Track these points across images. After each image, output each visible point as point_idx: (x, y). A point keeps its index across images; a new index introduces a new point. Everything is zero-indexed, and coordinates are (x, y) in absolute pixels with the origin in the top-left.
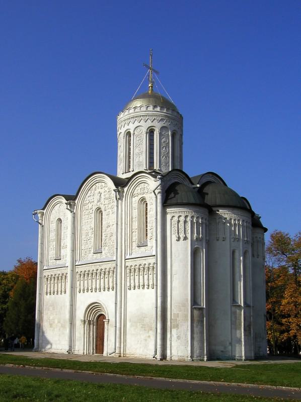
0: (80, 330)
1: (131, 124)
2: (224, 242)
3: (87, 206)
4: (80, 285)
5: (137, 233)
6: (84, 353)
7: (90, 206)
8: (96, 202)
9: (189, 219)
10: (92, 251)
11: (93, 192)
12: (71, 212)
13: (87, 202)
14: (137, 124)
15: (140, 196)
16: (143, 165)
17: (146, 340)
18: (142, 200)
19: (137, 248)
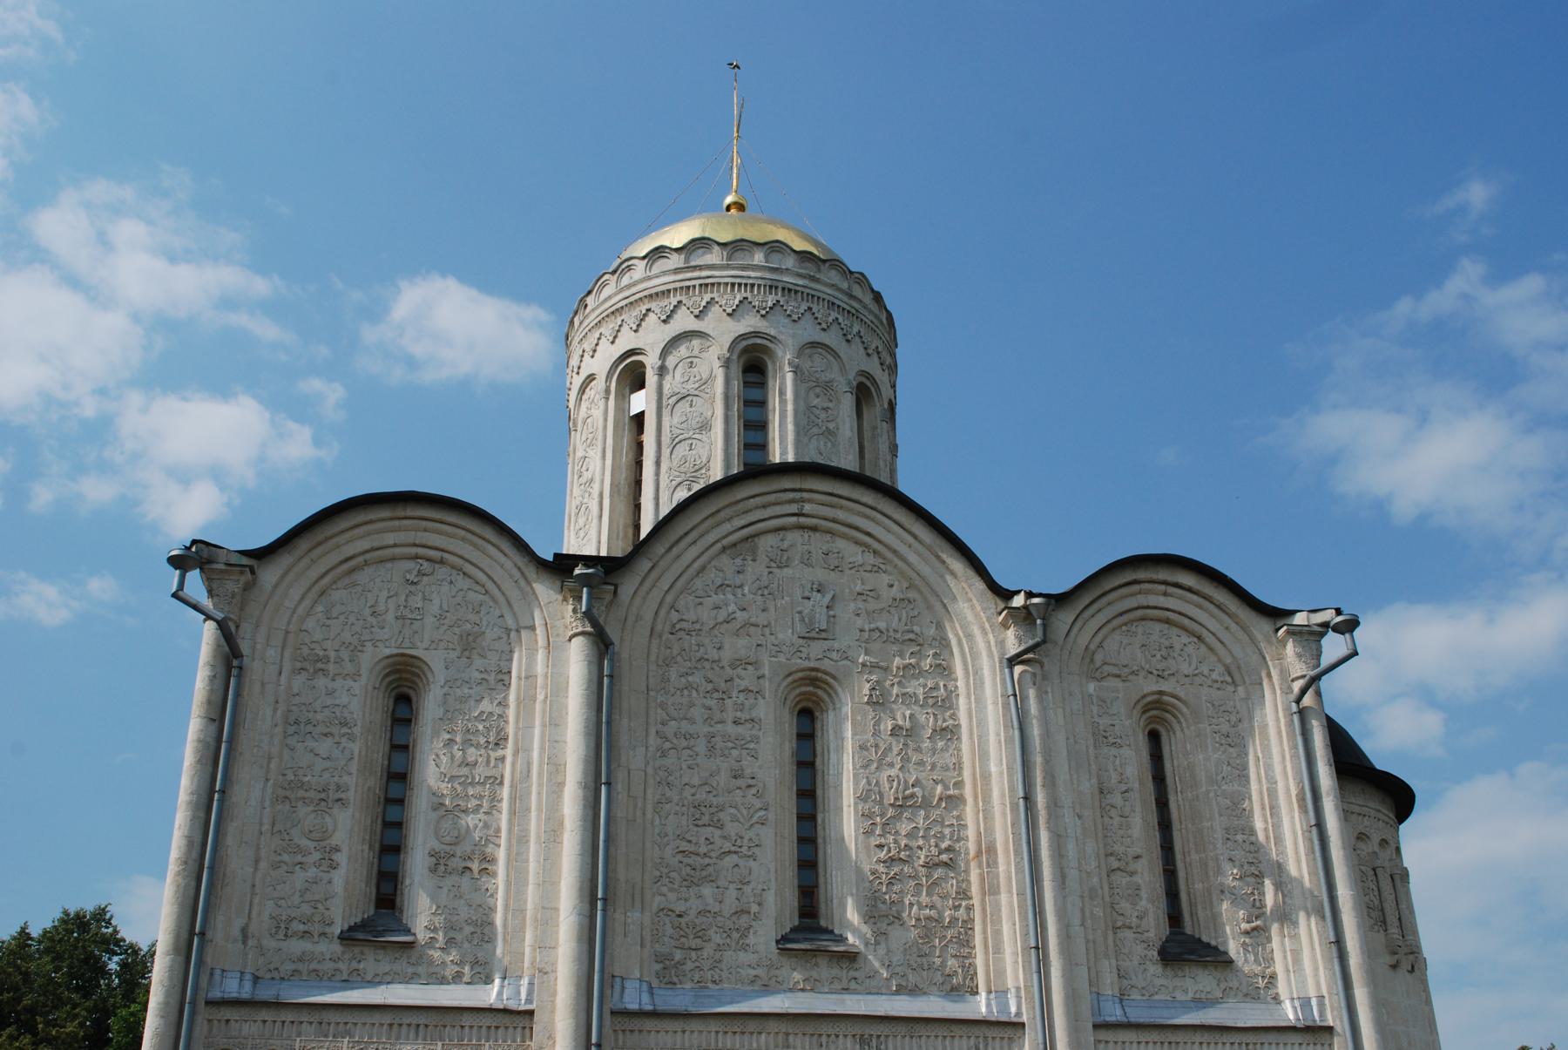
8: (786, 635)
11: (756, 570)
15: (1151, 686)
19: (1155, 969)
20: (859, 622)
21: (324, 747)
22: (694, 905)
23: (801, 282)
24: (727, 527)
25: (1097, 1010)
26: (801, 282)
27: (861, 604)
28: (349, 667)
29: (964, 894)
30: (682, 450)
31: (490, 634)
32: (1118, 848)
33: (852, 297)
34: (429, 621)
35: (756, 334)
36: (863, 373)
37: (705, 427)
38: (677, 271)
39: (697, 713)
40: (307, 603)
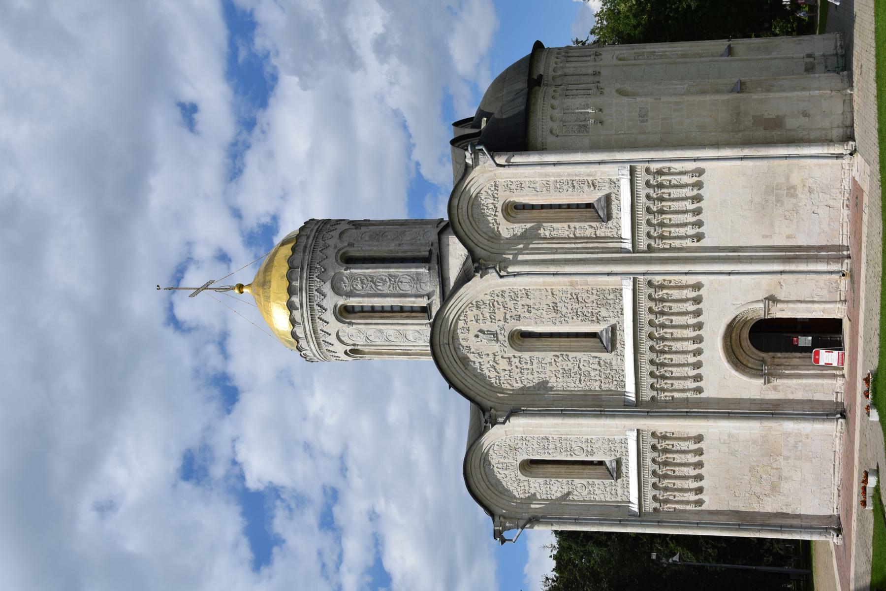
0: (792, 387)
1: (324, 303)
2: (603, 72)
3: (502, 374)
4: (683, 391)
5: (577, 225)
6: (840, 376)
7: (503, 364)
8: (496, 347)
9: (556, 103)
10: (605, 356)
12: (508, 418)
13: (493, 374)
14: (327, 288)
15: (500, 214)
16: (417, 274)
17: (811, 191)
18: (508, 214)
20: (488, 323)
21: (554, 488)
22: (598, 378)
23: (304, 295)
24: (458, 369)
25: (629, 252)
26: (304, 295)
27: (481, 322)
28: (526, 483)
29: (587, 291)
30: (391, 338)
31: (509, 442)
32: (567, 233)
33: (302, 269)
34: (506, 461)
35: (334, 313)
36: (337, 260)
37: (381, 331)
38: (308, 342)
39: (530, 377)
40: (505, 497)
